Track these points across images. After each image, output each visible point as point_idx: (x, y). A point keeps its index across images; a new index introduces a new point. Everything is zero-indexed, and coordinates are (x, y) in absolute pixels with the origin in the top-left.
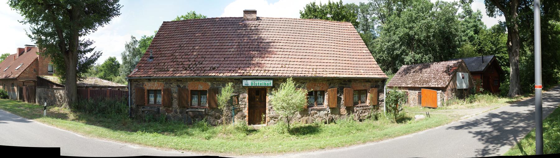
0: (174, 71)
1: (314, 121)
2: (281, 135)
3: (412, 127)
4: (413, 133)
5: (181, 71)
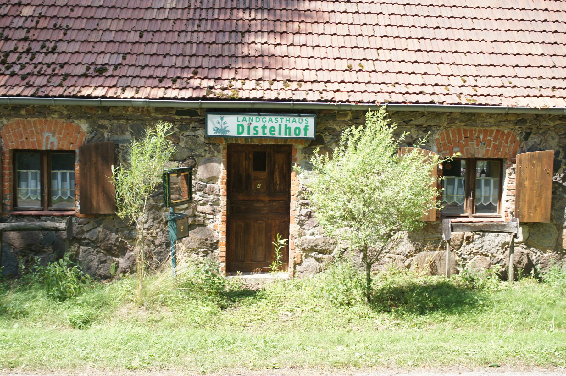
1: (460, 269)
2: (340, 310)
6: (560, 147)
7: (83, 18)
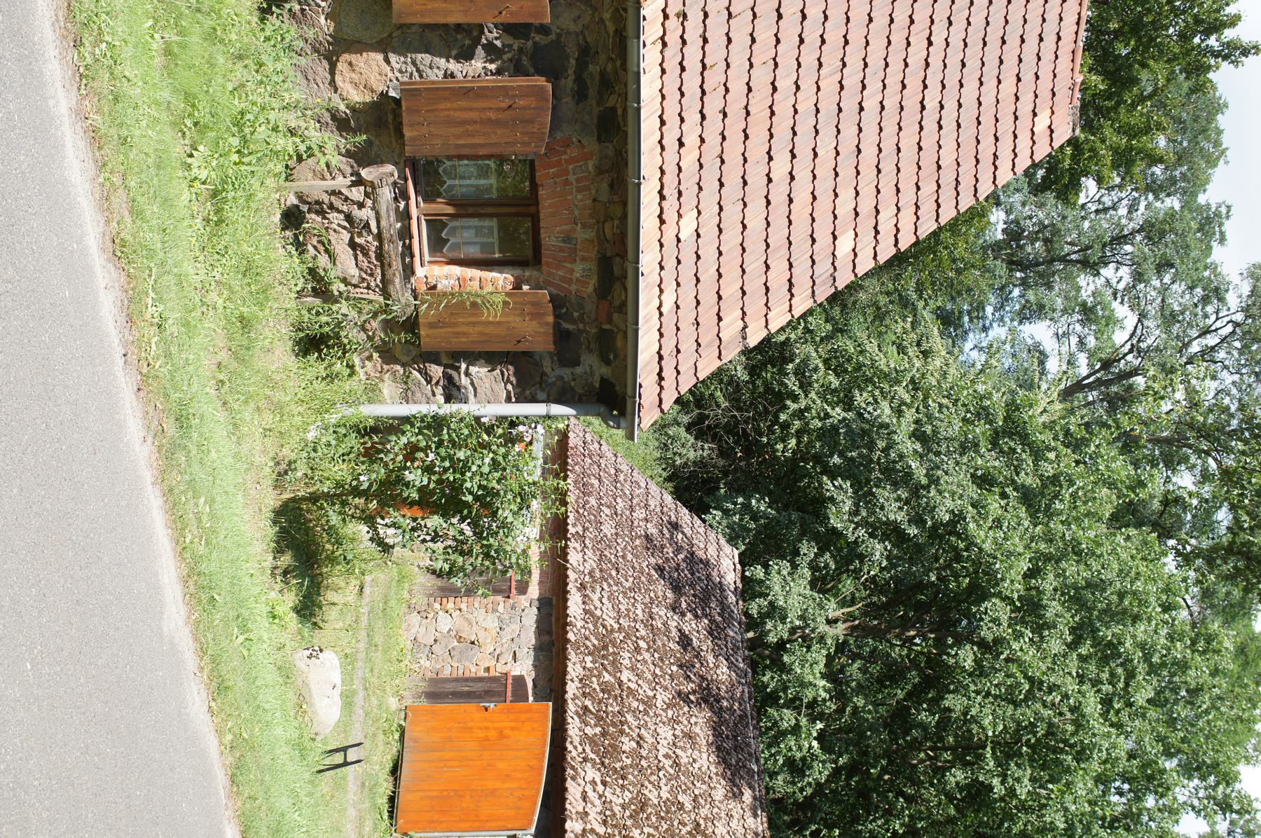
3: (244, 629)
4: (196, 639)
6: (559, 36)
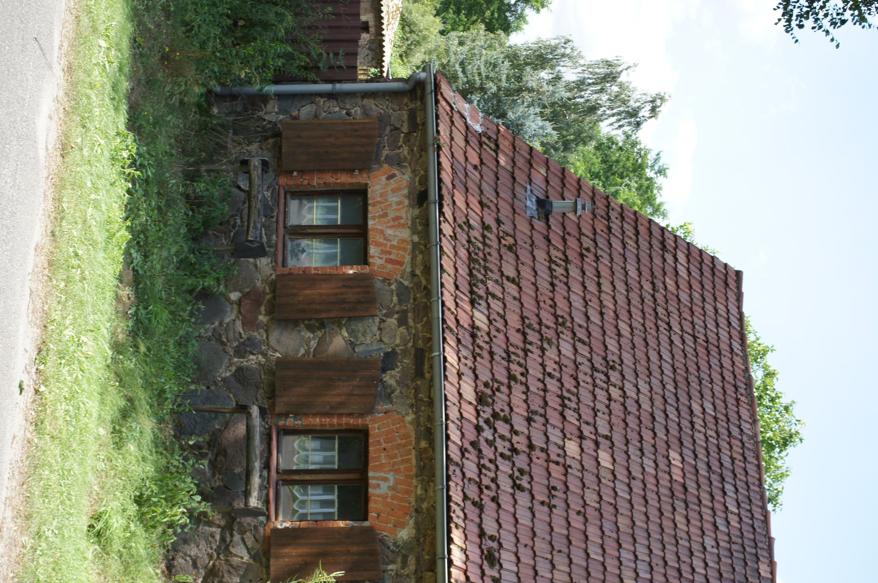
0: (473, 336)
5: (474, 370)
7: (568, 529)
